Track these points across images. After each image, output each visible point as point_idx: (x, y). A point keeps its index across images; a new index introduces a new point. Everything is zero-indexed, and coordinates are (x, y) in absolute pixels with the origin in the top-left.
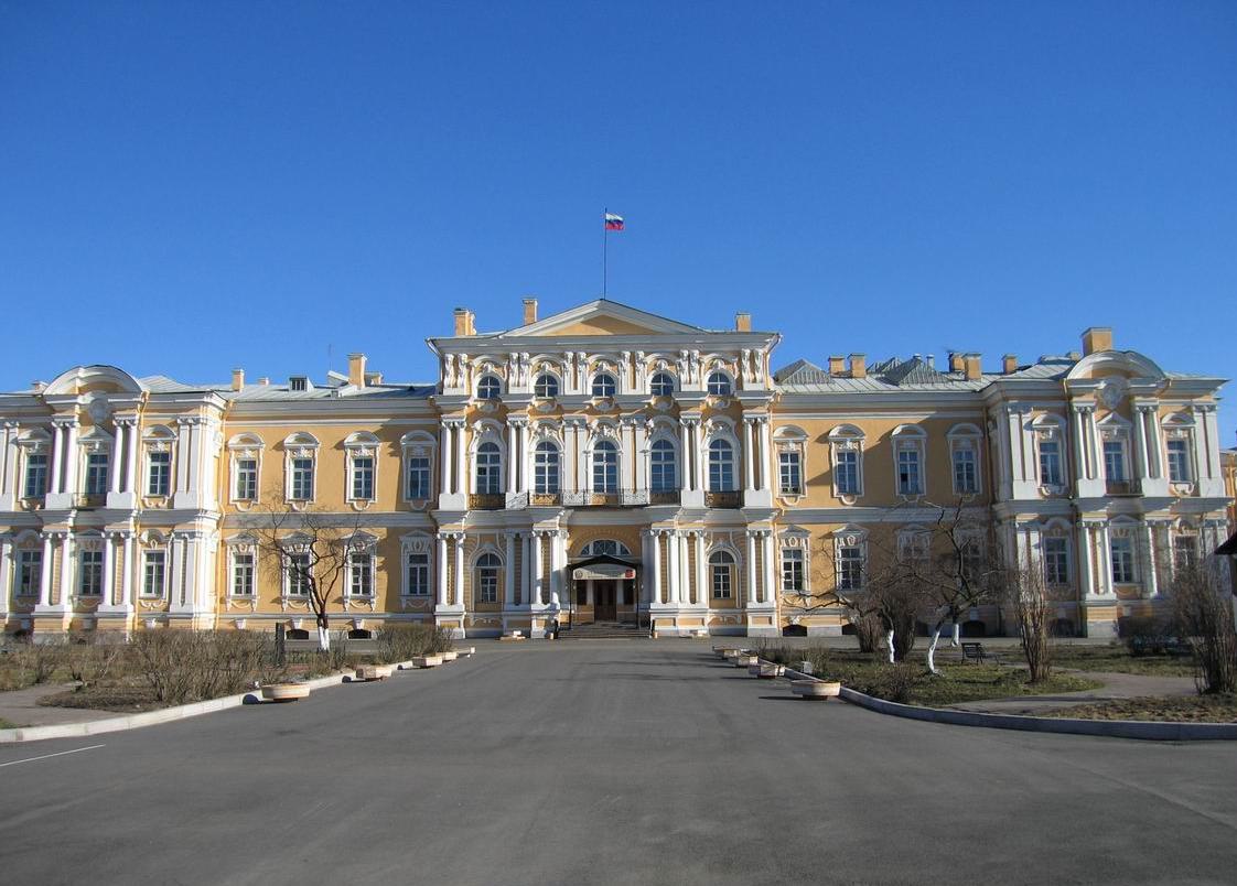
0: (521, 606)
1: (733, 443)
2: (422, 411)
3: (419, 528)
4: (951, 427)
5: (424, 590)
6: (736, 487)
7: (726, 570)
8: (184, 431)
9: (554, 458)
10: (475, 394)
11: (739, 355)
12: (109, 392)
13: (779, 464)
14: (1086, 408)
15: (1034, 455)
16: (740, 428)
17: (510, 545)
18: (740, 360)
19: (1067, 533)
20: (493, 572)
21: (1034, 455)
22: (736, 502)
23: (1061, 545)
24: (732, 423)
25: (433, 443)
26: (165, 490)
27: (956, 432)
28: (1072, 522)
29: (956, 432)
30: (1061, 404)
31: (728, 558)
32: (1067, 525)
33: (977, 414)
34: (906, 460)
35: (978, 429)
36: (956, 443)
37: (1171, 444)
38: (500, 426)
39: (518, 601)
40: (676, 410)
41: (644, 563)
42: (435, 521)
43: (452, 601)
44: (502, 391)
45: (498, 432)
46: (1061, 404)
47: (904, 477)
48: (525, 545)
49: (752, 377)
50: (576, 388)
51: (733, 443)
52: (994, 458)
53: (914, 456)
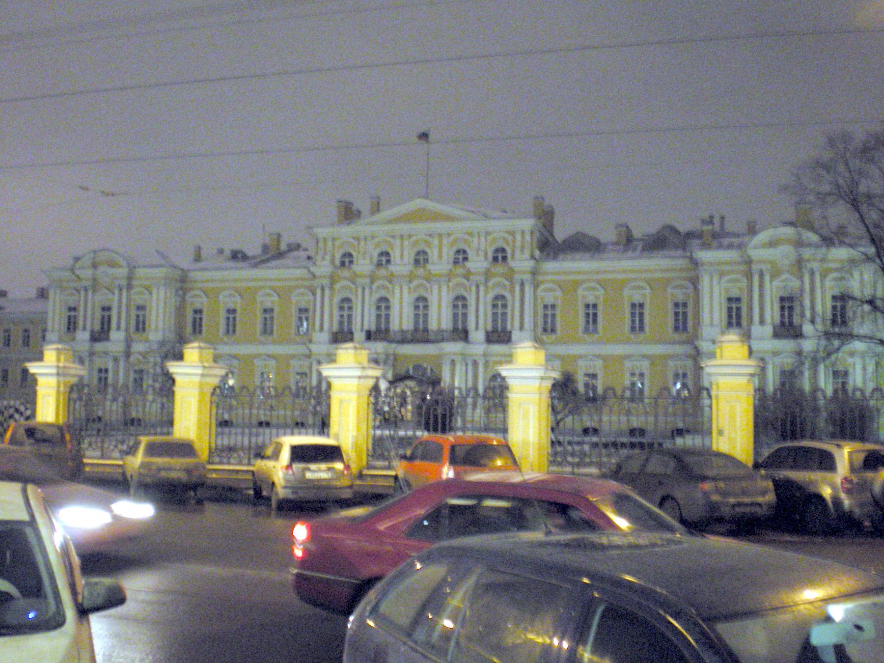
13: (725, 305)
16: (512, 283)
24: (507, 283)
25: (311, 297)
38: (353, 286)
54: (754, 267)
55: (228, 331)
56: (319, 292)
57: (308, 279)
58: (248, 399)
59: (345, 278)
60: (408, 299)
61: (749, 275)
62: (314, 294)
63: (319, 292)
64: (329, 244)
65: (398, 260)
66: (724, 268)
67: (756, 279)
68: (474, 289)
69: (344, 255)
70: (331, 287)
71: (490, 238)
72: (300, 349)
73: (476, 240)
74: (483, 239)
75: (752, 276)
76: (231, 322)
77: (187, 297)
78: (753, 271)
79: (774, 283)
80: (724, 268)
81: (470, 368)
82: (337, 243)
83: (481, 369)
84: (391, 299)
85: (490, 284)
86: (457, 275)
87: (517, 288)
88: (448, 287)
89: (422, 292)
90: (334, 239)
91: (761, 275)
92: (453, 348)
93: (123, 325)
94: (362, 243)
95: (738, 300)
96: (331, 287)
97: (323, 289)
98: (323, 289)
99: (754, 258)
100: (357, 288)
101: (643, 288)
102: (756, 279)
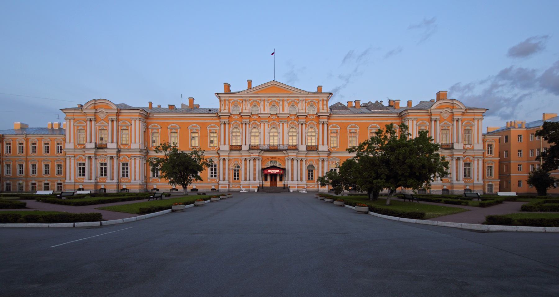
0: (247, 182)
5: (215, 176)
7: (312, 171)
11: (319, 101)
17: (243, 162)
20: (238, 171)
25: (218, 128)
31: (313, 166)
37: (465, 130)
39: (246, 180)
41: (286, 168)
42: (219, 154)
43: (224, 180)
48: (248, 162)
50: (264, 110)
56: (222, 126)
62: (220, 127)
73: (300, 103)
75: (431, 121)
79: (441, 124)
81: (299, 162)
83: (304, 162)
86: (292, 119)
87: (321, 125)
92: (292, 154)
93: (115, 140)
94: (244, 103)
96: (229, 124)
100: (242, 123)
102: (433, 122)
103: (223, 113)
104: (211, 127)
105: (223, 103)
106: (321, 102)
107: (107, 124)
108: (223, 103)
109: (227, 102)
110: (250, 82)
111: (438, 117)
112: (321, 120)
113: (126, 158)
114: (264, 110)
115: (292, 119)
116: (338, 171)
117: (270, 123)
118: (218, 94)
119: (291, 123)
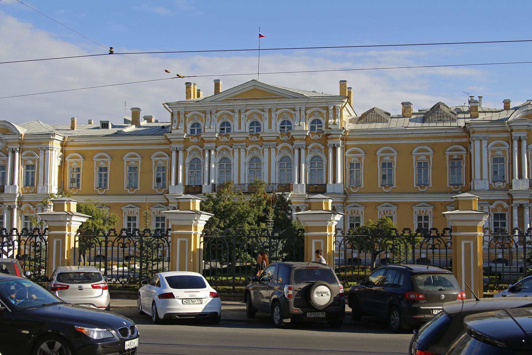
1: (324, 158)
2: (163, 141)
3: (160, 203)
4: (447, 148)
6: (325, 183)
8: (42, 152)
9: (229, 166)
10: (218, 130)
12: (5, 134)
14: (520, 137)
15: (488, 164)
16: (326, 148)
18: (328, 111)
19: (506, 210)
21: (488, 164)
22: (322, 190)
23: (503, 216)
24: (322, 147)
25: (167, 158)
26: (33, 184)
27: (450, 151)
28: (509, 204)
29: (450, 151)
30: (507, 135)
32: (505, 205)
33: (464, 140)
34: (386, 167)
35: (465, 150)
36: (450, 156)
40: (292, 140)
42: (167, 199)
44: (202, 131)
45: (200, 152)
46: (507, 135)
47: (158, 180)
49: (333, 121)
50: (240, 128)
51: (324, 158)
52: (46, 176)
53: (390, 165)
54: (514, 134)
55: (100, 185)
56: (174, 154)
57: (166, 144)
58: (104, 238)
59: (194, 144)
60: (245, 159)
61: (510, 141)
62: (170, 156)
63: (174, 154)
64: (182, 117)
65: (236, 130)
66: (491, 136)
67: (516, 143)
68: (296, 152)
69: (193, 126)
70: (185, 151)
71: (308, 112)
72: (159, 199)
74: (303, 113)
75: (512, 141)
76: (103, 178)
77: (67, 159)
78: (513, 138)
80: (491, 136)
82: (188, 116)
84: (232, 160)
85: (310, 147)
86: (283, 141)
88: (276, 149)
89: (255, 153)
90: (186, 113)
91: (520, 141)
94: (208, 116)
95: (502, 160)
97: (177, 152)
98: (177, 152)
99: (514, 128)
100: (204, 150)
101: (503, 145)
102: (516, 143)
103: (174, 135)
104: (157, 157)
105: (176, 117)
106: (331, 112)
107: (6, 157)
108: (176, 117)
109: (182, 117)
110: (217, 84)
111: (523, 134)
112: (330, 142)
113: (29, 209)
114: (240, 128)
115: (283, 141)
116: (289, 217)
117: (249, 148)
118: (167, 104)
119: (283, 148)
